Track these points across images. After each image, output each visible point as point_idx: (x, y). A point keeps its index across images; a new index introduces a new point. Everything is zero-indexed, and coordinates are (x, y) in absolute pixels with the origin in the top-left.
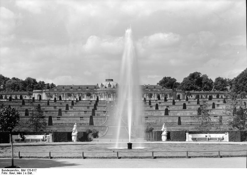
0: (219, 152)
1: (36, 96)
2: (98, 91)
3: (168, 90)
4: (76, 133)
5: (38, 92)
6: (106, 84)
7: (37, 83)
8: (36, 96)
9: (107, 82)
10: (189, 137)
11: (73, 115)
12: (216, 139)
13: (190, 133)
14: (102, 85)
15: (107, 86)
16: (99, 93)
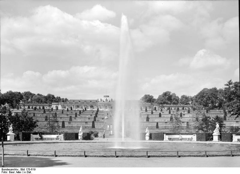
0: (206, 152)
1: (54, 107)
2: (97, 104)
3: (148, 104)
4: (82, 133)
5: (55, 104)
6: (104, 99)
7: (55, 98)
8: (54, 107)
9: (104, 98)
10: (166, 137)
11: (80, 120)
12: (186, 139)
13: (167, 134)
14: (101, 100)
15: (105, 101)
16: (99, 105)
